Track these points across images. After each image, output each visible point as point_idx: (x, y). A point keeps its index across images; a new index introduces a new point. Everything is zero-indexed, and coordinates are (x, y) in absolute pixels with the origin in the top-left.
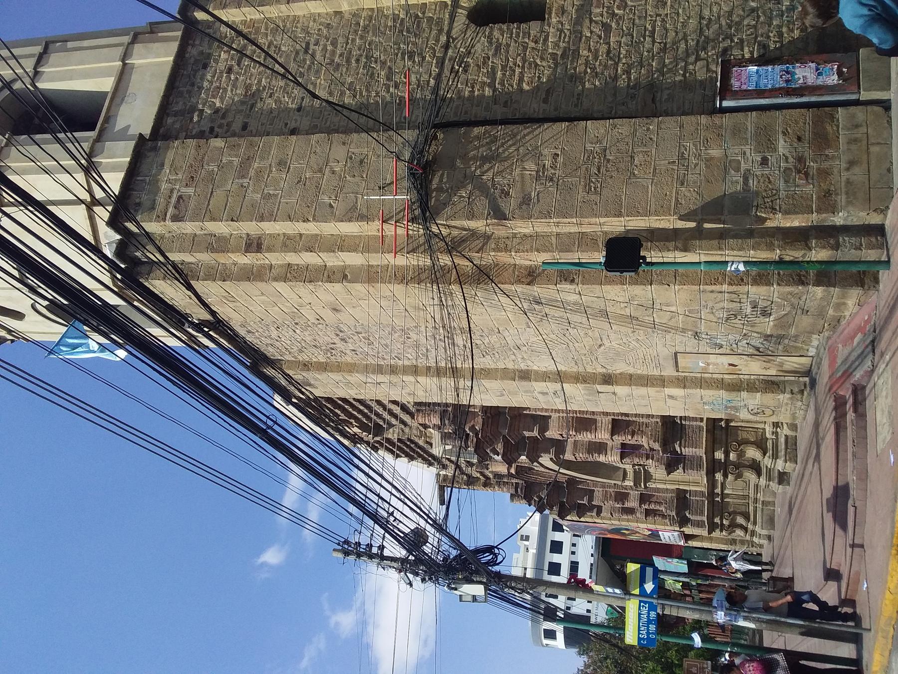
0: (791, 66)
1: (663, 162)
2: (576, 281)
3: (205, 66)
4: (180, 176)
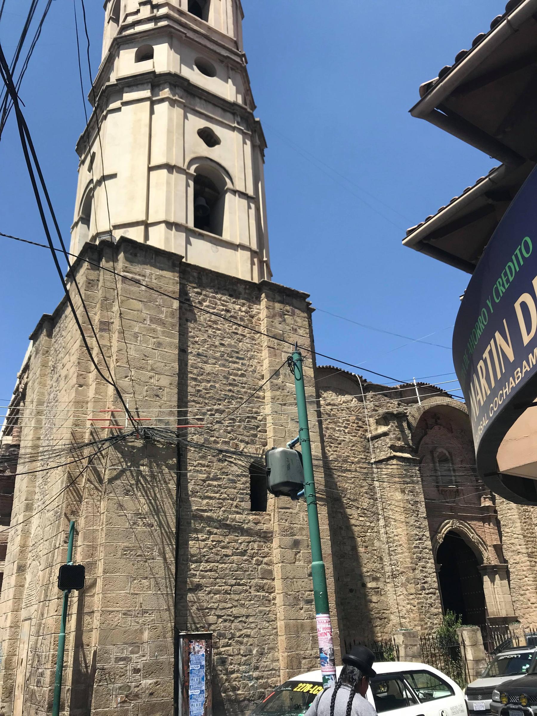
1: (141, 599)
2: (65, 545)
3: (231, 296)
4: (154, 281)
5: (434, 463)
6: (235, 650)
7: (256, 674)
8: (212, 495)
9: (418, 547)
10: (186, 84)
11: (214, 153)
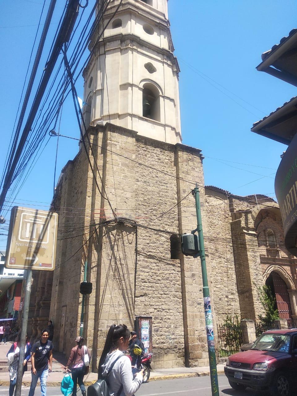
0: (148, 339)
5: (265, 236)
6: (163, 325)
7: (173, 337)
8: (152, 251)
9: (256, 279)
11: (154, 77)
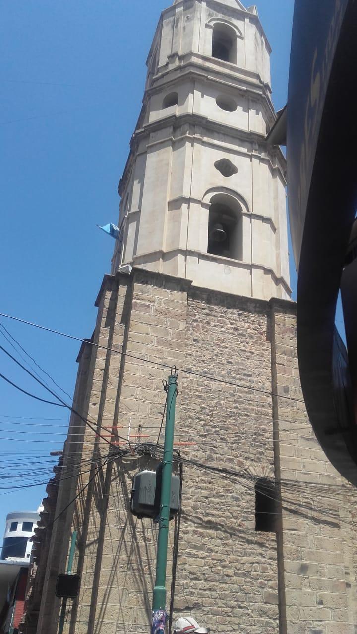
4: (163, 305)
8: (214, 512)
10: (204, 122)
11: (231, 182)
